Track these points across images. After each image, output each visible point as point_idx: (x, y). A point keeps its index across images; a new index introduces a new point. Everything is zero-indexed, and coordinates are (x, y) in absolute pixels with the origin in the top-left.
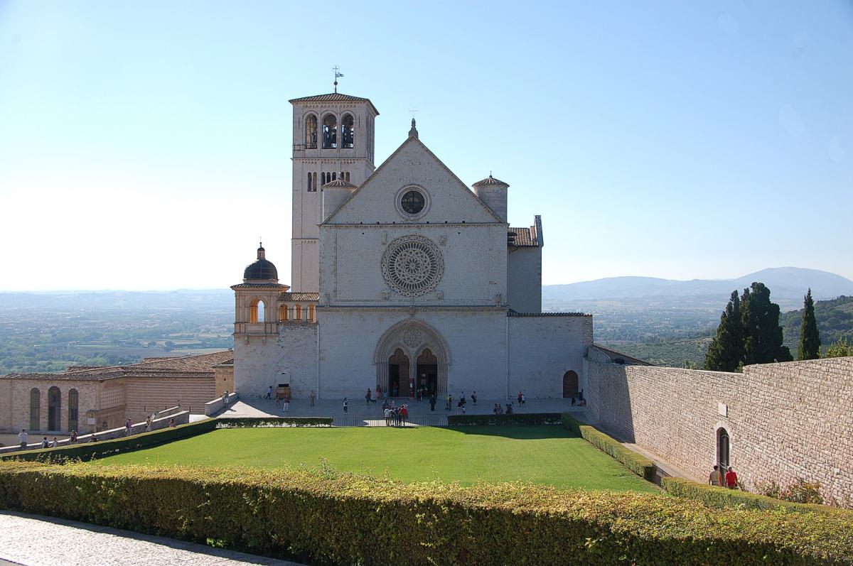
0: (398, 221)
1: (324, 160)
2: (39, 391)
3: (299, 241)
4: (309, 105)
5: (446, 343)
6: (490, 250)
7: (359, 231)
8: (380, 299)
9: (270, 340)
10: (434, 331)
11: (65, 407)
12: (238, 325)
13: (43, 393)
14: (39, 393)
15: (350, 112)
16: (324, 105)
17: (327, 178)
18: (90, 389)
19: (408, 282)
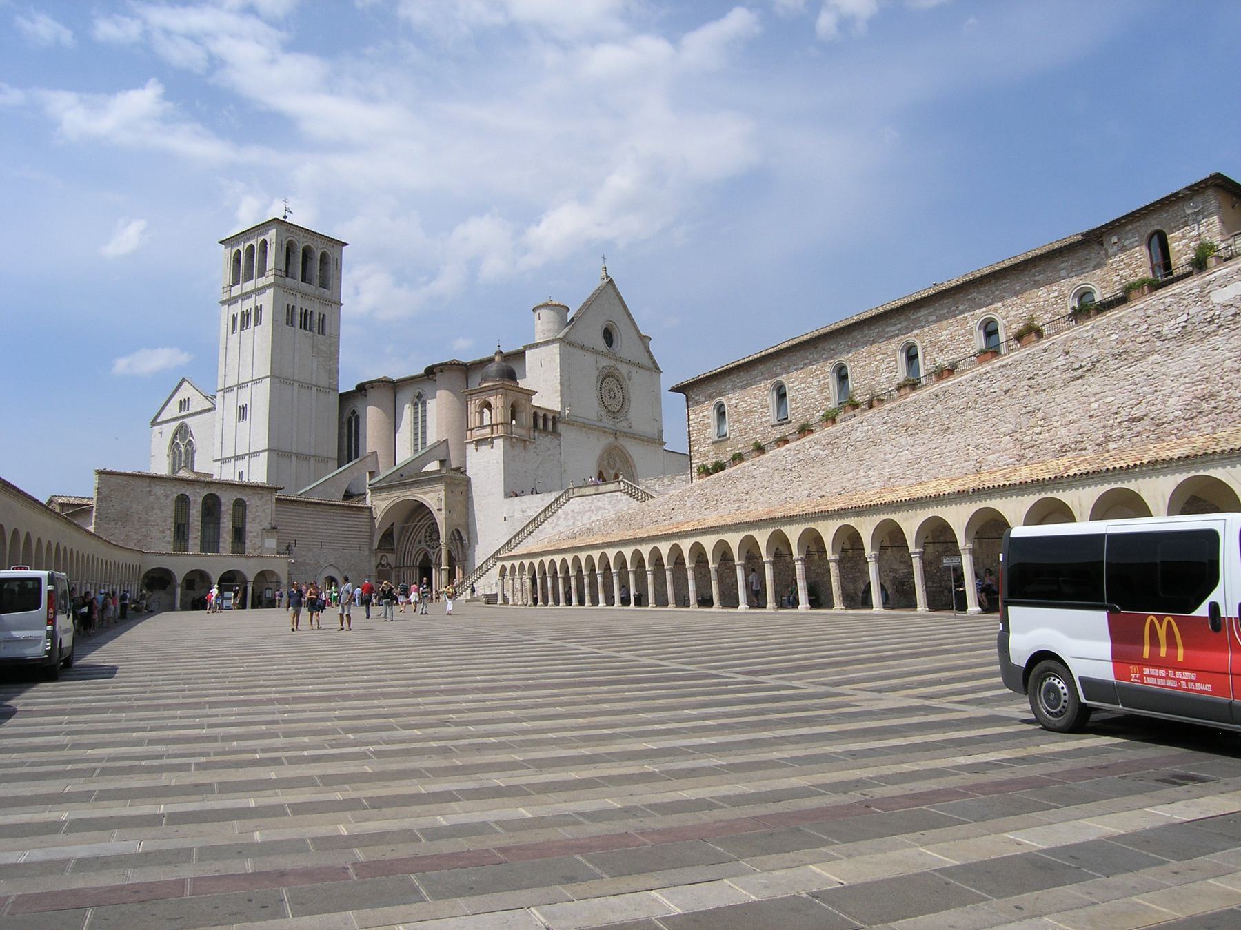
0: (605, 351)
1: (304, 295)
2: (187, 497)
3: (278, 380)
4: (291, 230)
5: (635, 468)
6: (653, 391)
7: (581, 352)
8: (596, 419)
9: (530, 446)
10: (628, 456)
11: (227, 524)
12: (505, 425)
13: (195, 502)
14: (189, 502)
15: (328, 252)
16: (305, 235)
17: (306, 316)
18: (263, 500)
19: (610, 408)
